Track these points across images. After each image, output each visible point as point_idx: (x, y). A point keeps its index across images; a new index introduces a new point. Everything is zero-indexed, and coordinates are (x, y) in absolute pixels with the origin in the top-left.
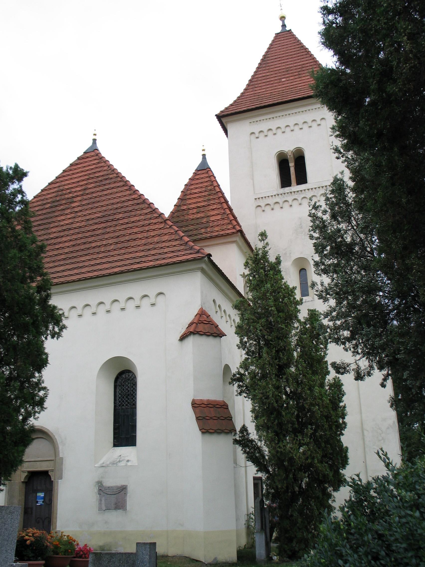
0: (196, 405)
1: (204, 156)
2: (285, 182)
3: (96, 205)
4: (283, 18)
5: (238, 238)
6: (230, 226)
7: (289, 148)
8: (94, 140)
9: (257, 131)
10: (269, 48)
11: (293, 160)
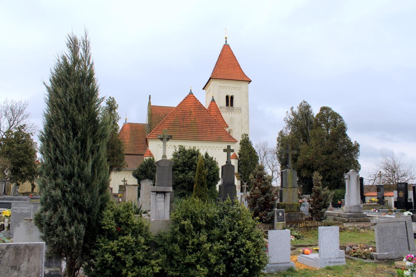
2: (227, 105)
4: (226, 38)
7: (230, 95)
8: (191, 90)
9: (221, 86)
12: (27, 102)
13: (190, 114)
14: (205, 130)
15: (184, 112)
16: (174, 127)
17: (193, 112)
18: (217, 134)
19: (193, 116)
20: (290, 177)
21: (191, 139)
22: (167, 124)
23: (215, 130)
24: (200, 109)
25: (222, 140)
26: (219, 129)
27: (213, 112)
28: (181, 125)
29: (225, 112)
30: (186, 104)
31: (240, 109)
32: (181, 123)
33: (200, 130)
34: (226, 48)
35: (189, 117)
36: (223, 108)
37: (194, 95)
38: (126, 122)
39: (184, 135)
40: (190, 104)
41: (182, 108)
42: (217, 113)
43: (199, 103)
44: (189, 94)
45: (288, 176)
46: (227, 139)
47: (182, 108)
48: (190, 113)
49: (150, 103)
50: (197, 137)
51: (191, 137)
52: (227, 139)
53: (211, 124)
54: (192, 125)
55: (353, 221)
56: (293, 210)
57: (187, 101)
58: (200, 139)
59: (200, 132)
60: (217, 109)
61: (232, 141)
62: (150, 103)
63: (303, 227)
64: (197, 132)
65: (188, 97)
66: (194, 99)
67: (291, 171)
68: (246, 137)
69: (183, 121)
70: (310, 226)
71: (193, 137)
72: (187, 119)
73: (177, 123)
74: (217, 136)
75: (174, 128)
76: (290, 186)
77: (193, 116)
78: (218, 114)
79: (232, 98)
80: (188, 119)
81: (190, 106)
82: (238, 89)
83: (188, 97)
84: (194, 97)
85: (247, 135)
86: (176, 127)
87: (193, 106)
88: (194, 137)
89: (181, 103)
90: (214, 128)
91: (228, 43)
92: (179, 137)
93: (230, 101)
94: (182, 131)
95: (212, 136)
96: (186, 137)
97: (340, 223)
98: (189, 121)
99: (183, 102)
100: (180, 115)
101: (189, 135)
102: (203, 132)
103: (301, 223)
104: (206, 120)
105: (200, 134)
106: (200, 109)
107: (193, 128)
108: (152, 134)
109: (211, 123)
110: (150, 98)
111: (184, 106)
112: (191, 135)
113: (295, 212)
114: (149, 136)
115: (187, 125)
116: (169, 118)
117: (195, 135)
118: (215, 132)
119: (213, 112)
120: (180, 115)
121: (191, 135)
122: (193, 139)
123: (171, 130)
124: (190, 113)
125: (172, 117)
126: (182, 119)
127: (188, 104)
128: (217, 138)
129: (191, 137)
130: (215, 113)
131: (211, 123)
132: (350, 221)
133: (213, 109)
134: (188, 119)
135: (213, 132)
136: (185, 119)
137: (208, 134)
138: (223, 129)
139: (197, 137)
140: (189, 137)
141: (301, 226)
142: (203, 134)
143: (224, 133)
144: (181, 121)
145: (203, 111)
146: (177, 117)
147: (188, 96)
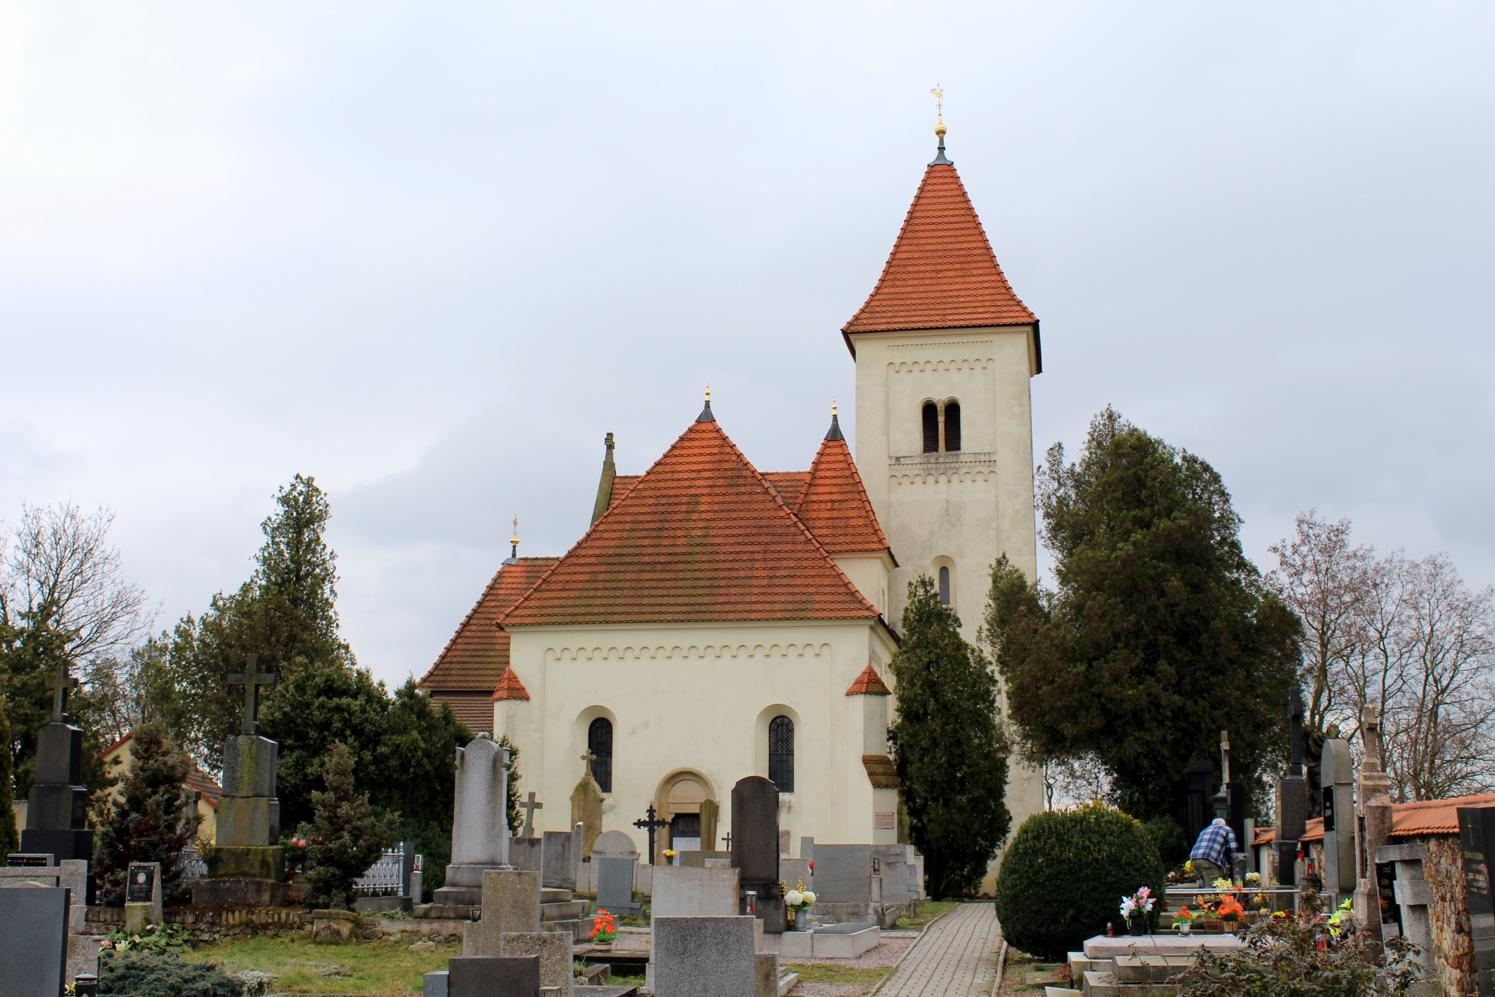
0: (867, 761)
1: (835, 417)
2: (930, 444)
3: (734, 515)
4: (941, 133)
5: (884, 555)
7: (940, 397)
8: (707, 403)
9: (897, 362)
10: (918, 198)
12: (104, 510)
13: (690, 508)
15: (664, 501)
16: (616, 568)
18: (791, 590)
19: (703, 516)
20: (247, 762)
21: (677, 617)
22: (588, 560)
23: (786, 572)
24: (735, 481)
25: (809, 614)
26: (805, 563)
28: (646, 559)
29: (918, 480)
30: (678, 468)
31: (989, 461)
32: (649, 550)
34: (941, 179)
35: (684, 524)
36: (908, 461)
37: (719, 423)
38: (514, 555)
39: (653, 600)
40: (694, 467)
41: (662, 484)
42: (849, 488)
43: (734, 458)
44: (698, 422)
45: (240, 759)
46: (832, 606)
47: (662, 484)
48: (689, 503)
49: (609, 465)
50: (704, 608)
51: (678, 609)
52: (832, 606)
53: (772, 548)
54: (690, 558)
55: (445, 914)
56: (246, 869)
57: (684, 452)
58: (716, 616)
59: (722, 583)
60: (847, 473)
62: (609, 465)
63: (240, 925)
64: (708, 583)
65: (692, 436)
66: (717, 442)
67: (253, 741)
68: (927, 592)
69: (657, 542)
70: (263, 921)
71: (685, 609)
72: (672, 533)
73: (631, 551)
74: (789, 598)
76: (245, 790)
77: (703, 516)
78: (849, 496)
79: (953, 409)
80: (679, 533)
81: (694, 475)
82: (978, 366)
83: (692, 436)
84: (718, 431)
86: (623, 568)
88: (690, 609)
89: (657, 464)
90: (785, 564)
91: (949, 155)
93: (941, 425)
94: (647, 584)
95: (768, 599)
96: (657, 609)
97: (338, 914)
98: (679, 541)
99: (668, 460)
100: (649, 518)
101: (672, 600)
102: (735, 582)
103: (233, 913)
104: (755, 531)
105: (721, 591)
106: (735, 481)
108: (526, 604)
109: (777, 539)
110: (610, 446)
111: (669, 476)
112: (679, 600)
113: (254, 875)
114: (507, 616)
115: (669, 559)
116: (598, 535)
117: (699, 600)
120: (649, 518)
121: (679, 600)
122: (684, 617)
123: (601, 585)
124: (689, 503)
125: (615, 527)
126: (655, 533)
127: (686, 468)
128: (790, 607)
129: (678, 609)
130: (835, 489)
131: (777, 539)
132: (433, 914)
133: (829, 474)
134: (679, 533)
135: (776, 581)
136: (665, 533)
137: (755, 591)
138: (822, 563)
139: (704, 608)
140: (671, 609)
141: (231, 921)
142: (733, 591)
143: (827, 581)
144: (646, 542)
145: (749, 489)
146: (634, 526)
147: (690, 430)
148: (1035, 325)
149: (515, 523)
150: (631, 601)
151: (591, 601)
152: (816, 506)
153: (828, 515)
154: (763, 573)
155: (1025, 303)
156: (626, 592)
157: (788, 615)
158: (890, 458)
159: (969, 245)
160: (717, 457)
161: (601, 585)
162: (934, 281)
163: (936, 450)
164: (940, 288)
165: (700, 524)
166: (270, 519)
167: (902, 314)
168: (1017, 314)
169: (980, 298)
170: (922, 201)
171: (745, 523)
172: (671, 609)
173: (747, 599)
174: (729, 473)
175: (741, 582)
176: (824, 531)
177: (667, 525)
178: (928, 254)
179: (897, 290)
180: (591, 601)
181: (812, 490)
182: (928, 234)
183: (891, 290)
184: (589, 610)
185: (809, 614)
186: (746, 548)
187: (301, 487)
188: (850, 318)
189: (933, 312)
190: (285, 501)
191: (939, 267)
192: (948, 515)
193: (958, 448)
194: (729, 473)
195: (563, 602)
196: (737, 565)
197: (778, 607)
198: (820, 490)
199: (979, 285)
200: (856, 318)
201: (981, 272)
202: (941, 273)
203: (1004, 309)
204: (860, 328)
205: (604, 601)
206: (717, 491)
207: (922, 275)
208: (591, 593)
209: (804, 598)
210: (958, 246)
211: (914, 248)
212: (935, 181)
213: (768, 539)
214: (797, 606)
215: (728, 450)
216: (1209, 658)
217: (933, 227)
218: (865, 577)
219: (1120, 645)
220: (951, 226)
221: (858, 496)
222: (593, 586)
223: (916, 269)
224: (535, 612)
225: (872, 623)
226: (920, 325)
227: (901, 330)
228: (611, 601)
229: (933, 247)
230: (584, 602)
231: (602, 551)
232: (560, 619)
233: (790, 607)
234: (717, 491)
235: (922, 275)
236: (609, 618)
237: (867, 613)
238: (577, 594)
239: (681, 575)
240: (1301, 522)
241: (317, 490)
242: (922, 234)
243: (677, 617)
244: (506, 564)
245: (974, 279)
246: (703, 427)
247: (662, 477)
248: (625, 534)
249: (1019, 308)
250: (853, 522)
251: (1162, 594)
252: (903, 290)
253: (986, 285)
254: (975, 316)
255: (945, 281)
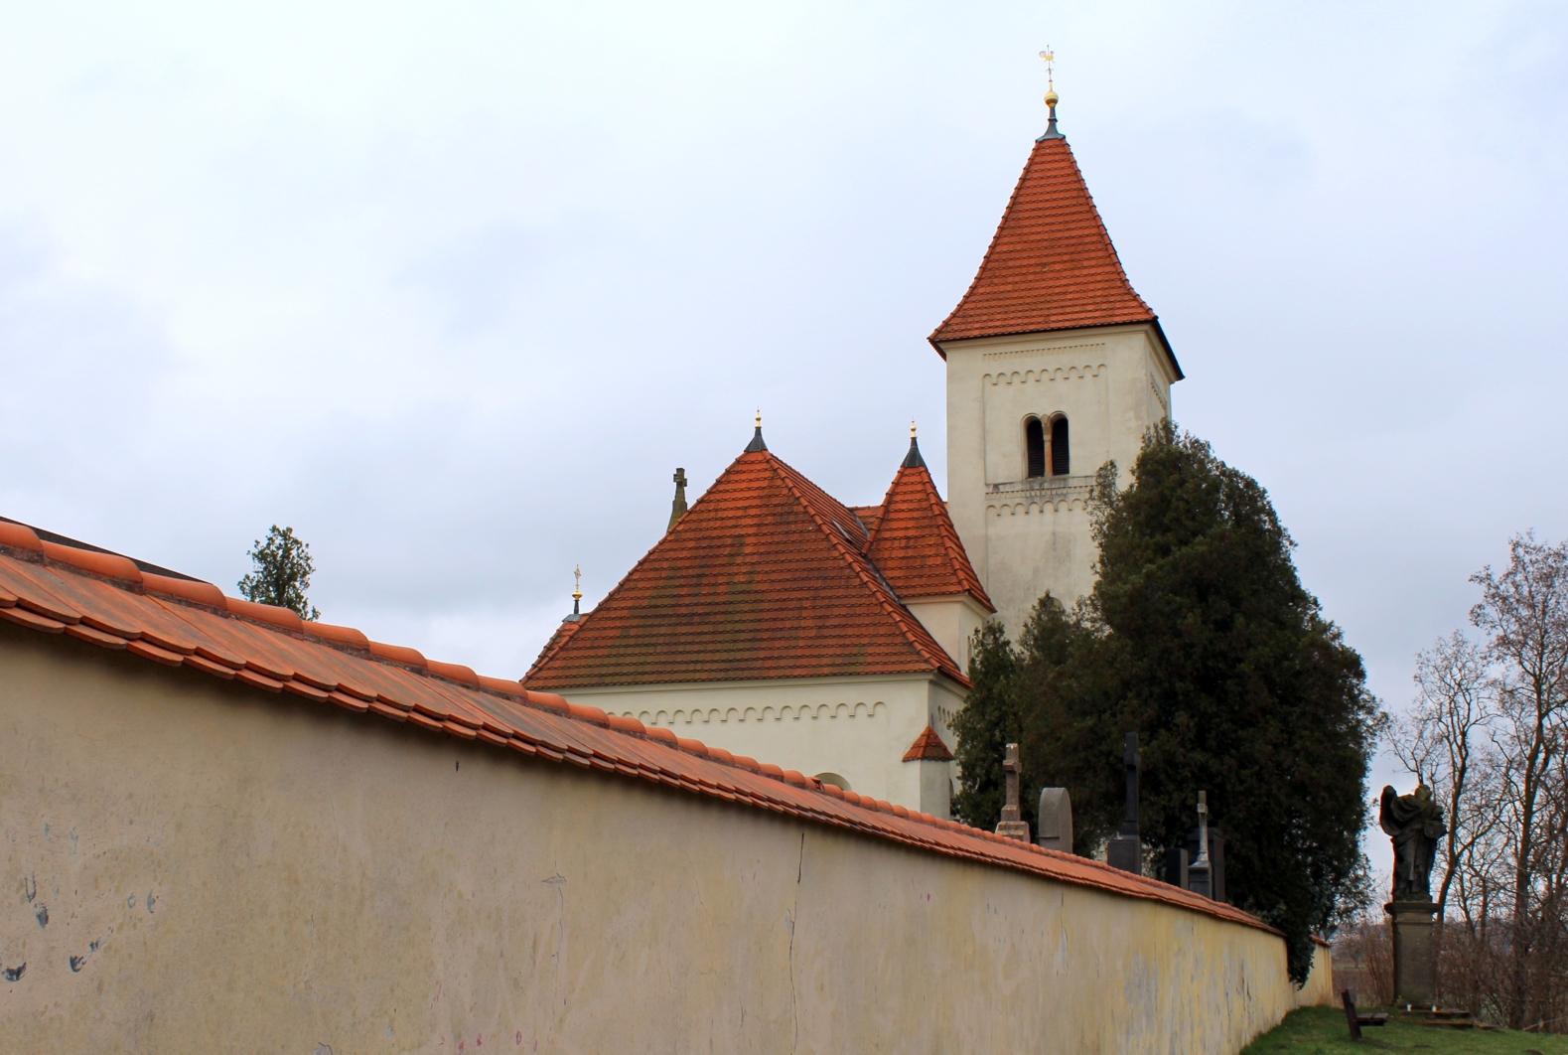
1: (914, 440)
2: (1035, 467)
4: (1052, 102)
6: (954, 579)
7: (1044, 411)
8: (758, 430)
10: (1023, 180)
11: (1050, 430)
13: (734, 550)
14: (788, 624)
15: (704, 544)
17: (749, 540)
18: (841, 641)
19: (748, 560)
21: (713, 675)
22: (619, 613)
23: (836, 622)
25: (859, 669)
26: (858, 610)
27: (903, 524)
28: (684, 610)
29: (1020, 510)
30: (723, 505)
32: (687, 601)
33: (765, 625)
36: (1008, 488)
38: (576, 610)
40: (740, 504)
42: (926, 522)
43: (785, 491)
44: (747, 451)
46: (885, 659)
47: (704, 524)
50: (743, 665)
51: (715, 666)
52: (885, 659)
53: (823, 593)
58: (756, 673)
59: (765, 635)
61: (910, 667)
66: (768, 474)
68: (996, 639)
69: (696, 590)
73: (666, 601)
74: (839, 651)
75: (649, 631)
78: (927, 531)
79: (1060, 424)
80: (721, 580)
81: (740, 513)
83: (740, 468)
85: (1002, 632)
86: (657, 621)
87: (752, 512)
90: (836, 611)
91: (1061, 128)
92: (660, 668)
94: (683, 639)
95: (816, 652)
96: (691, 667)
98: (721, 589)
99: (712, 497)
101: (708, 657)
102: (779, 634)
104: (805, 574)
105: (764, 645)
107: (737, 617)
108: (551, 664)
111: (712, 515)
112: (717, 656)
115: (707, 609)
116: (632, 584)
117: (738, 655)
118: (837, 632)
119: (903, 524)
120: (688, 563)
121: (717, 656)
122: (721, 675)
123: (632, 641)
124: (732, 545)
125: (651, 575)
128: (839, 661)
130: (910, 524)
131: (829, 583)
133: (904, 506)
135: (825, 632)
136: (704, 581)
137: (801, 643)
138: (877, 610)
139: (743, 665)
140: (708, 666)
144: (684, 591)
145: (800, 527)
147: (738, 461)
148: (1154, 322)
149: (577, 574)
150: (663, 658)
151: (621, 660)
152: (888, 544)
153: (902, 553)
154: (810, 623)
155: (1143, 298)
156: (659, 649)
157: (836, 670)
158: (987, 485)
159: (1080, 233)
160: (766, 492)
161: (632, 641)
162: (1038, 277)
163: (1041, 473)
164: (1044, 284)
165: (744, 569)
166: (247, 577)
167: (999, 317)
168: (1131, 311)
169: (1091, 294)
170: (1028, 184)
171: (794, 566)
172: (708, 666)
173: (792, 653)
174: (779, 509)
175: (786, 634)
176: (896, 573)
177: (706, 571)
178: (1033, 245)
179: (996, 289)
180: (621, 660)
181: (885, 526)
182: (1033, 222)
183: (988, 289)
184: (617, 669)
185: (859, 669)
186: (794, 595)
187: (279, 540)
188: (938, 324)
189: (1035, 313)
190: (262, 556)
191: (1045, 260)
192: (1054, 550)
193: (1067, 472)
194: (779, 509)
195: (590, 662)
196: (781, 615)
197: (825, 661)
198: (894, 525)
199: (1090, 279)
200: (946, 324)
201: (1093, 263)
202: (1049, 268)
203: (1118, 305)
204: (950, 336)
205: (635, 660)
206: (765, 530)
207: (1024, 271)
208: (622, 651)
209: (855, 650)
210: (1067, 234)
211: (1017, 239)
212: (1044, 159)
213: (819, 583)
214: (847, 660)
215: (779, 482)
216: (1237, 708)
217: (1040, 213)
218: (950, 628)
219: (1130, 695)
220: (1060, 211)
221: (936, 531)
222: (624, 642)
223: (1018, 263)
224: (560, 673)
225: (931, 677)
226: (1019, 329)
227: (996, 335)
228: (642, 659)
229: (1038, 237)
230: (613, 660)
231: (637, 603)
232: (586, 681)
233: (839, 661)
234: (765, 530)
235: (1024, 271)
236: (639, 678)
237: (924, 666)
238: (606, 652)
239: (721, 628)
240: (1516, 545)
241: (296, 542)
242: (1027, 223)
243: (713, 675)
244: (567, 622)
245: (1085, 272)
246: (752, 457)
247: (705, 516)
248: (661, 583)
249: (1135, 304)
250: (930, 561)
251: (1178, 634)
252: (1002, 288)
253: (1099, 278)
254: (1083, 315)
255: (1050, 275)
